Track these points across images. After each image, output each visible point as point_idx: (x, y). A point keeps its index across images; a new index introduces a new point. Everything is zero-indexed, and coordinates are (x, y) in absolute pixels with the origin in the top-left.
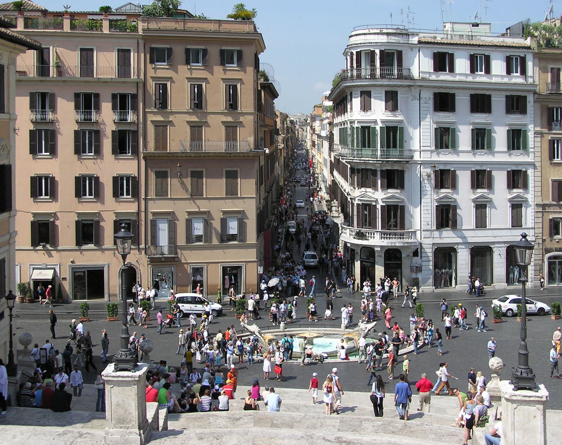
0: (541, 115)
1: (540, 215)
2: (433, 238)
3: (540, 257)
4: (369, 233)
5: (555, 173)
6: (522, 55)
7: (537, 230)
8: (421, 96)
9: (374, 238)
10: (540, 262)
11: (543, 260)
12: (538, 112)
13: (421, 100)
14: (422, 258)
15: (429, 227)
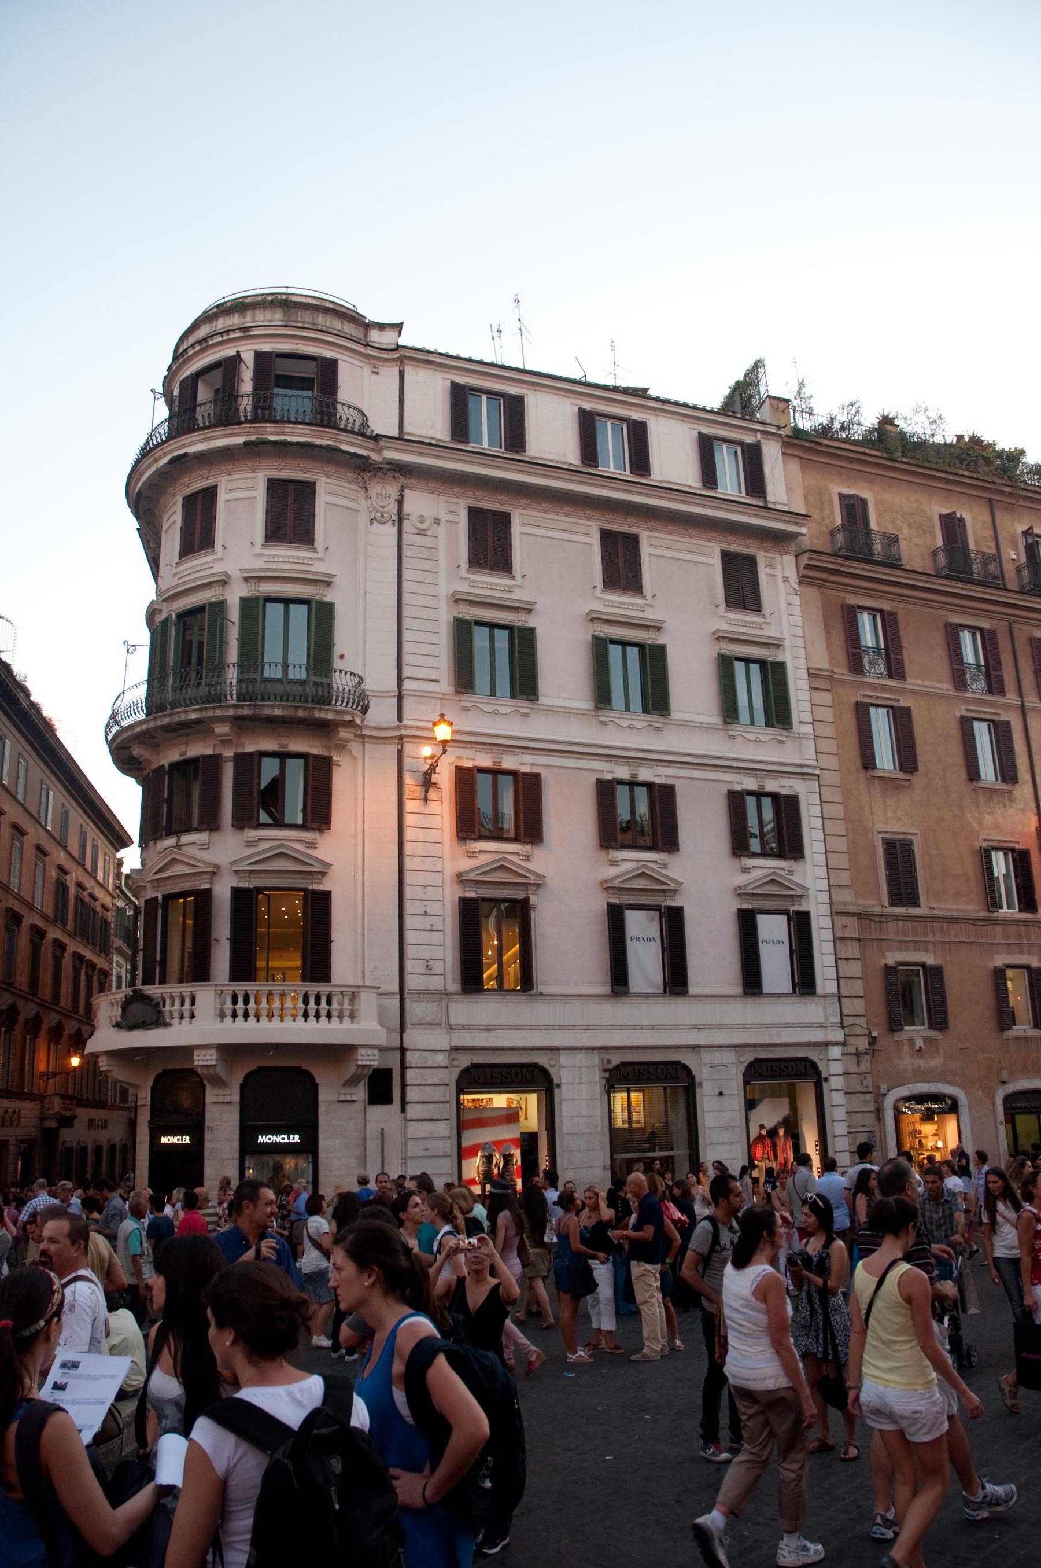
0: (826, 626)
1: (852, 950)
2: (451, 1028)
3: (866, 1103)
4: (172, 999)
5: (890, 814)
6: (749, 439)
7: (849, 1006)
8: (407, 509)
9: (192, 1016)
10: (870, 1119)
11: (879, 1113)
12: (817, 614)
13: (406, 524)
14: (412, 1111)
15: (436, 983)
